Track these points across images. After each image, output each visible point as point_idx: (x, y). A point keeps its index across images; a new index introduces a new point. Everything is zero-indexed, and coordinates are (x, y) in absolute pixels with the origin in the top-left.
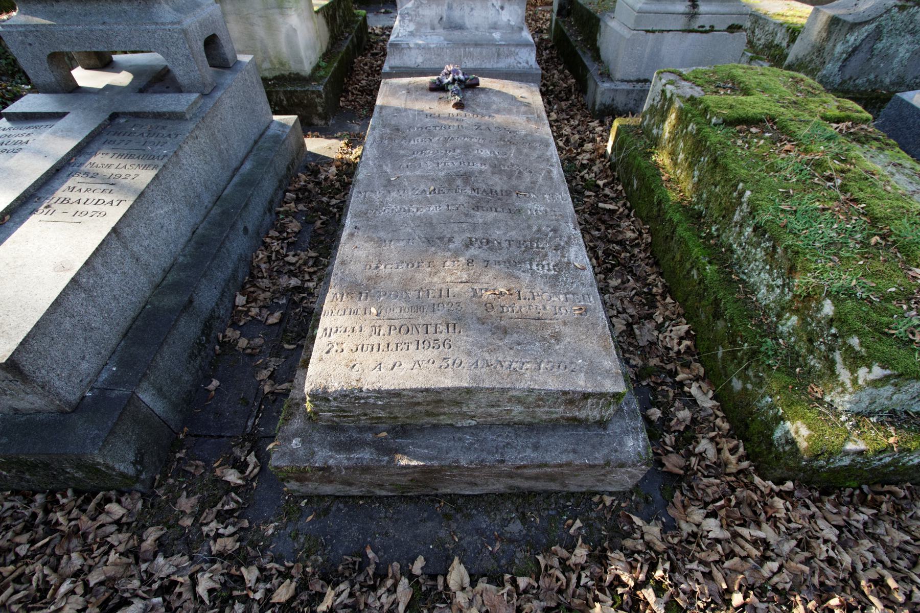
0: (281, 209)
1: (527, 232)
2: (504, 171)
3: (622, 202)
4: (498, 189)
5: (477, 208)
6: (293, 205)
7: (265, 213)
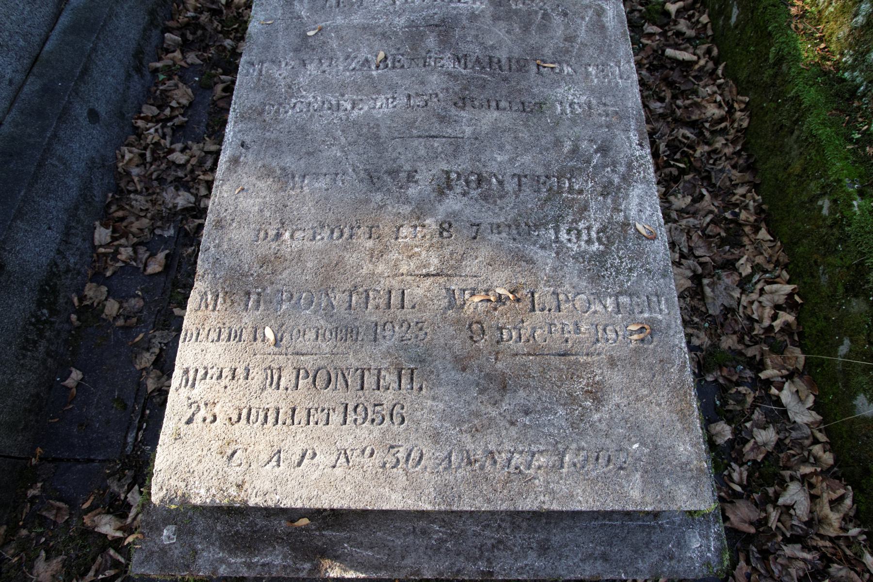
0: (159, 65)
1: (552, 155)
2: (516, 12)
3: (705, 47)
4: (502, 55)
5: (463, 101)
6: (177, 55)
7: (129, 76)
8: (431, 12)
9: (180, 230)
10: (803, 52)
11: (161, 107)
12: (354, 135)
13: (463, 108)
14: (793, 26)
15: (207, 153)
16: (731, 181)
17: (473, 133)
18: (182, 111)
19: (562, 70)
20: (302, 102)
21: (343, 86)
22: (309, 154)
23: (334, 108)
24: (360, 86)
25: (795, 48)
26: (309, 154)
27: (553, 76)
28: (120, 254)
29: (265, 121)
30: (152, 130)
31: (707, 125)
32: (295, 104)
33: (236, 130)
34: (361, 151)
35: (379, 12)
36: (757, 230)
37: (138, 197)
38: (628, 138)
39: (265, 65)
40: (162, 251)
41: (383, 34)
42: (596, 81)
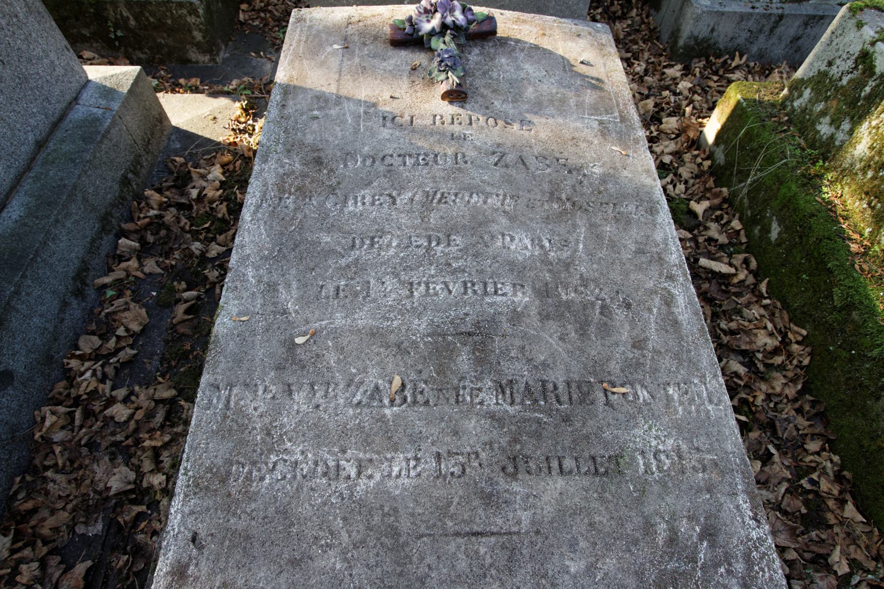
0: (107, 280)
1: (643, 553)
2: (568, 305)
3: (741, 257)
4: (557, 376)
5: (514, 464)
6: (133, 263)
8: (461, 312)
9: (111, 523)
10: (877, 303)
11: (104, 337)
12: (361, 527)
13: (514, 476)
14: (857, 267)
15: (158, 402)
16: (798, 430)
17: (533, 523)
18: (131, 341)
19: (636, 395)
20: (285, 461)
21: (344, 432)
22: (294, 563)
23: (332, 475)
24: (368, 436)
25: (867, 297)
26: (294, 563)
27: (627, 407)
28: (20, 573)
29: (229, 495)
30: (88, 374)
31: (760, 356)
32: (275, 464)
33: (187, 510)
34: (372, 561)
35: (392, 308)
36: (842, 503)
37: (59, 477)
38: (738, 507)
39: (235, 391)
40: (82, 561)
41: (398, 346)
42: (680, 409)
